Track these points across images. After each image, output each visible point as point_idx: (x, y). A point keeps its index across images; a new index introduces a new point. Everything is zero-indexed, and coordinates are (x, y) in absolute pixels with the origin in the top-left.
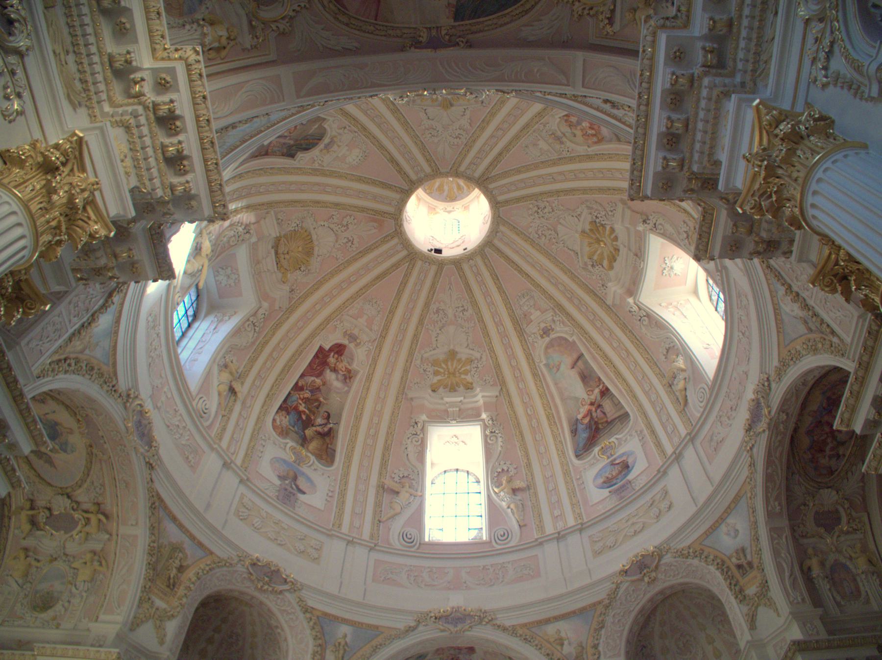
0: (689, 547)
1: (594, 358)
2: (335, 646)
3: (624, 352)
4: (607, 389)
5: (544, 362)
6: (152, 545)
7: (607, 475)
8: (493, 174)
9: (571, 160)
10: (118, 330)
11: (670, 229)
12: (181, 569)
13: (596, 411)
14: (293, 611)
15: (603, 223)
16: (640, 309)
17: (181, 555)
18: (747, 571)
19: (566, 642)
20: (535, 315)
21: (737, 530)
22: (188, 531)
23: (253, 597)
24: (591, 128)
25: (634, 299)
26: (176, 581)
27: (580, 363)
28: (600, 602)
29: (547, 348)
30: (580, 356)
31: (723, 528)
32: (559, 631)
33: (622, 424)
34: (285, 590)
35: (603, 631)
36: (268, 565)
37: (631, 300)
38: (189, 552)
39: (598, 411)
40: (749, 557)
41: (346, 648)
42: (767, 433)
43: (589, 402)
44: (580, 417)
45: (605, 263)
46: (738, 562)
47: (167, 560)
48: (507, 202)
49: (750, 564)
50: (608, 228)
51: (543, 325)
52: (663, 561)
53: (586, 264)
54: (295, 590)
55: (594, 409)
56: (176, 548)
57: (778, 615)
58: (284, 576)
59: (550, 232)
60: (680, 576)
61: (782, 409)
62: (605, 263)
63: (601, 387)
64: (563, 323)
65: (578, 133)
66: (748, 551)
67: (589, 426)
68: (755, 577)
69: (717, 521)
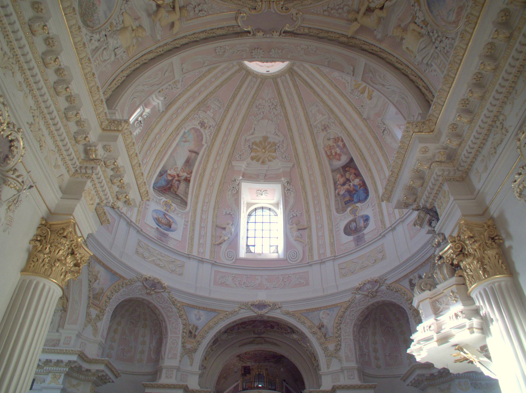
0: (179, 302)
1: (200, 163)
3: (212, 183)
4: (189, 181)
5: (186, 131)
7: (160, 217)
8: (296, 78)
9: (312, 134)
11: (291, 201)
13: (176, 181)
15: (277, 151)
16: (238, 185)
18: (192, 337)
19: (98, 281)
20: (210, 113)
21: (200, 319)
24: (336, 153)
25: (241, 179)
27: (194, 154)
28: (124, 278)
29: (194, 128)
30: (197, 153)
31: (196, 311)
32: (99, 272)
33: (181, 204)
35: (116, 294)
37: (241, 178)
39: (177, 182)
40: (197, 333)
42: (255, 314)
43: (178, 173)
44: (169, 172)
45: (253, 154)
46: (191, 330)
48: (277, 84)
49: (195, 336)
50: (274, 154)
51: (206, 121)
52: (162, 293)
53: (249, 140)
55: (176, 178)
57: (191, 365)
59: (262, 113)
60: (161, 305)
61: (269, 317)
62: (253, 154)
63: (188, 176)
64: (211, 133)
65: (331, 143)
66: (198, 331)
67: (168, 182)
68: (193, 343)
69: (197, 307)
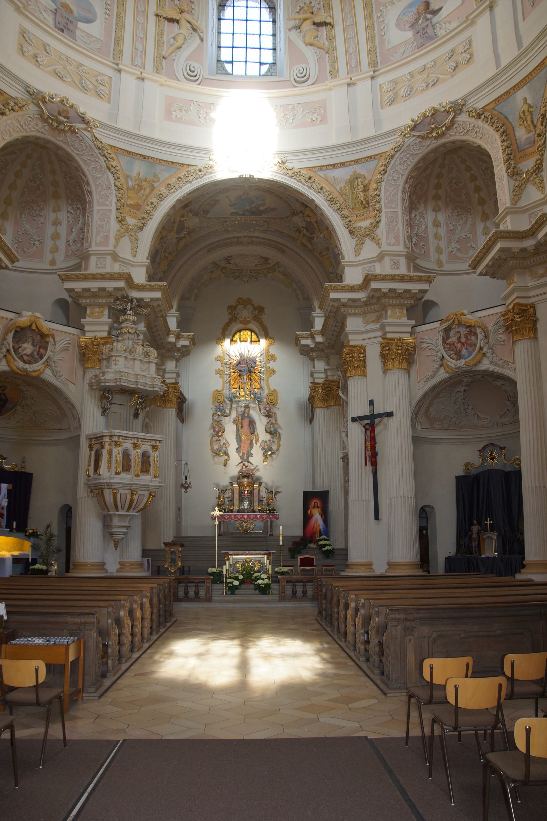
2: (521, 117)
6: (329, 198)
10: (152, 157)
12: (366, 189)
14: (472, 125)
17: (359, 180)
22: (352, 161)
23: (444, 145)
26: (367, 199)
34: (454, 117)
36: (425, 116)
38: (364, 173)
41: (531, 110)
47: (353, 193)
54: (461, 110)
56: (352, 181)
58: (443, 109)
